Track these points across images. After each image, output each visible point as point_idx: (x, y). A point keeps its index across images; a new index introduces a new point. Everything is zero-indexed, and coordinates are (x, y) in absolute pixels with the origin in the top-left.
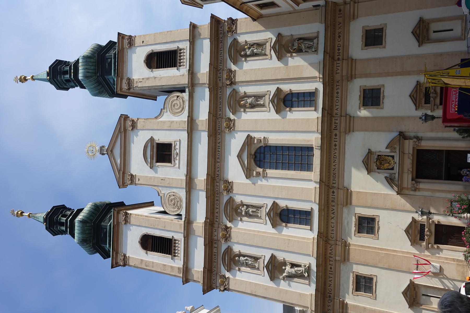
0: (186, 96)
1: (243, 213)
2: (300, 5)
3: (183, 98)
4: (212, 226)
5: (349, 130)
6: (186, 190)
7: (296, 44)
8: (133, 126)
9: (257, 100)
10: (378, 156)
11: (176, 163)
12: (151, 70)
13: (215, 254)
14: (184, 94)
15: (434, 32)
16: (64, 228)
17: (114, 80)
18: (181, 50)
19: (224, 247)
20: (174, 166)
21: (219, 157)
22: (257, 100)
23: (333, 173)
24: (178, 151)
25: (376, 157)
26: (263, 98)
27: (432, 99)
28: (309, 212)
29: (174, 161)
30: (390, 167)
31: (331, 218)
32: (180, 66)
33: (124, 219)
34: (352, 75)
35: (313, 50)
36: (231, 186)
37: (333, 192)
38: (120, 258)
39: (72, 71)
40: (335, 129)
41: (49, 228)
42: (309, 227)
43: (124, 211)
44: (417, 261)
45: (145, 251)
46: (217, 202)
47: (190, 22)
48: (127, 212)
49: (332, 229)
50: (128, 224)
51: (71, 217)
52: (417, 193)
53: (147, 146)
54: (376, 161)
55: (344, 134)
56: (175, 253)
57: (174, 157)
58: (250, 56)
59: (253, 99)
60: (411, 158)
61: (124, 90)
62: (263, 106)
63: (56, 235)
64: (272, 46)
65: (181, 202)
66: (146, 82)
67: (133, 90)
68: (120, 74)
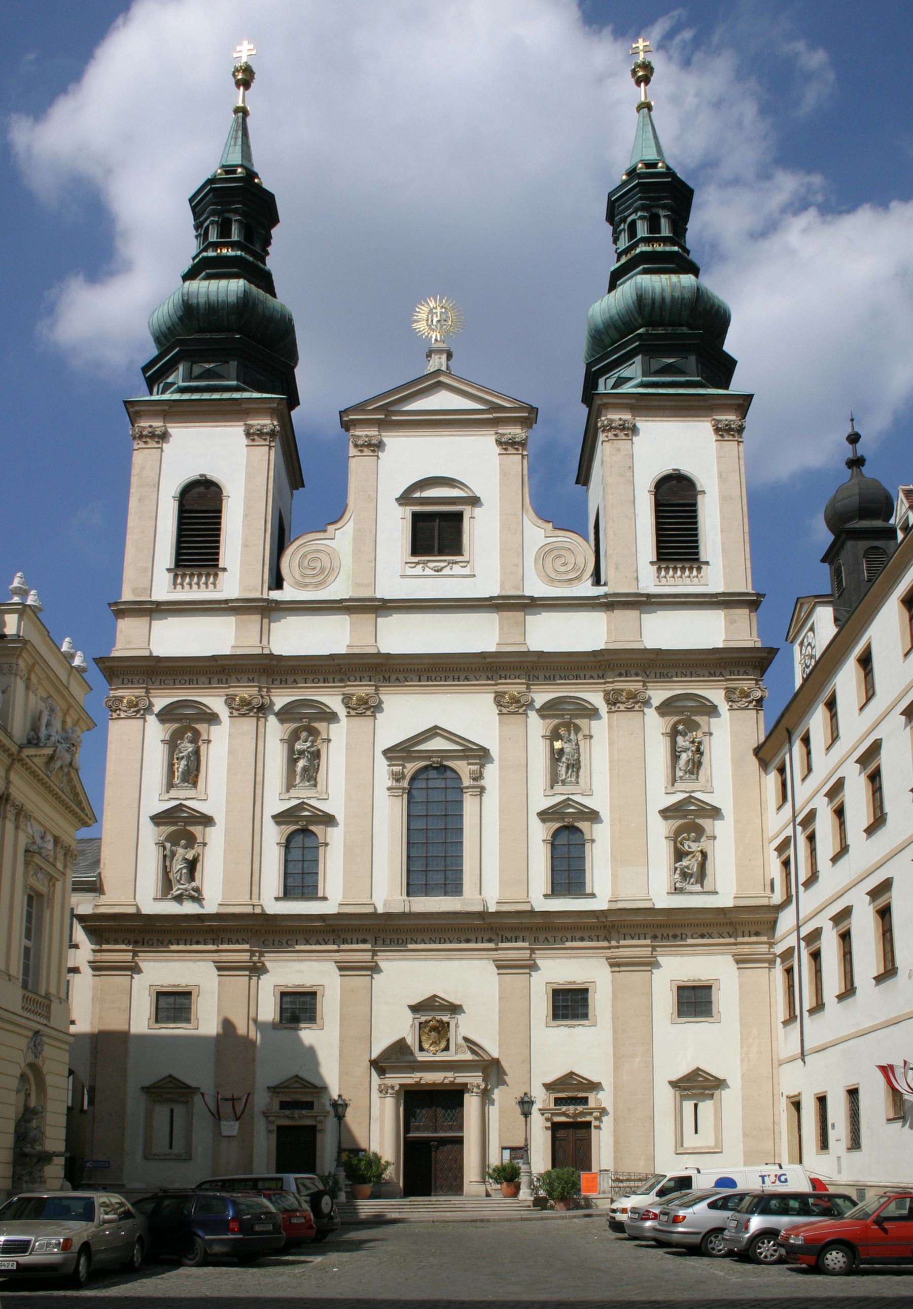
0: (586, 589)
1: (298, 746)
2: (776, 853)
3: (578, 578)
4: (262, 670)
5: (501, 966)
6: (345, 600)
7: (694, 847)
8: (506, 443)
9: (571, 766)
10: (448, 1023)
11: (415, 567)
12: (652, 489)
13: (195, 682)
14: (590, 582)
15: (696, 1106)
16: (213, 237)
17: (630, 379)
18: (699, 569)
19: (215, 702)
20: (407, 563)
21: (433, 678)
22: (571, 766)
23: (406, 939)
24: (444, 572)
25: (445, 1019)
26: (573, 779)
27: (564, 1108)
28: (317, 893)
29: (418, 563)
30: (426, 1046)
31: (308, 939)
32: (659, 569)
33: (258, 430)
34: (618, 965)
35: (678, 885)
36: (364, 713)
37: (364, 941)
38: (158, 424)
39: (659, 248)
40: (504, 938)
41: (212, 190)
42: (281, 895)
43: (278, 428)
44: (239, 1099)
45: (178, 495)
46: (322, 680)
47: (765, 595)
48: (278, 437)
49: (284, 942)
50: (244, 441)
51: (251, 259)
52: (375, 1094)
53: (454, 487)
54: (437, 1021)
55: (493, 956)
56: (184, 576)
57: (429, 561)
58: (674, 743)
59: (572, 756)
60: (446, 1081)
61: (604, 412)
62: (554, 780)
63: (193, 209)
64: (692, 794)
65: (315, 587)
66: (621, 475)
67: (603, 441)
68: (643, 403)
